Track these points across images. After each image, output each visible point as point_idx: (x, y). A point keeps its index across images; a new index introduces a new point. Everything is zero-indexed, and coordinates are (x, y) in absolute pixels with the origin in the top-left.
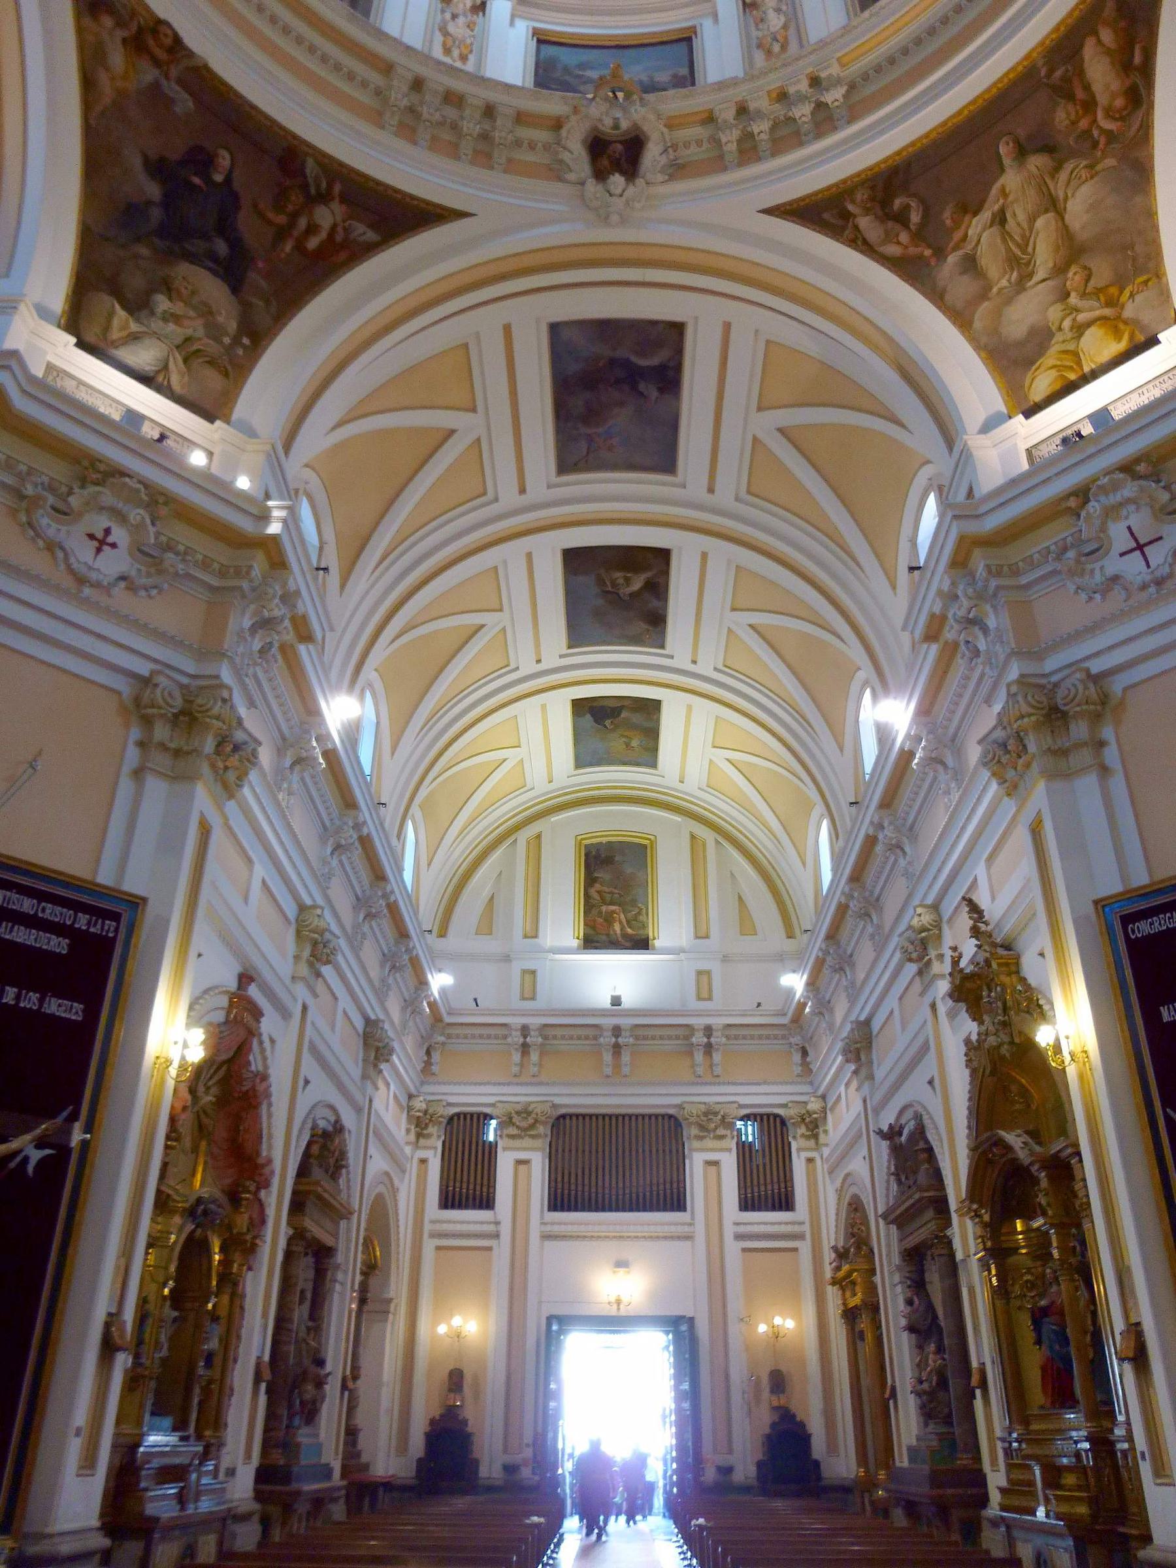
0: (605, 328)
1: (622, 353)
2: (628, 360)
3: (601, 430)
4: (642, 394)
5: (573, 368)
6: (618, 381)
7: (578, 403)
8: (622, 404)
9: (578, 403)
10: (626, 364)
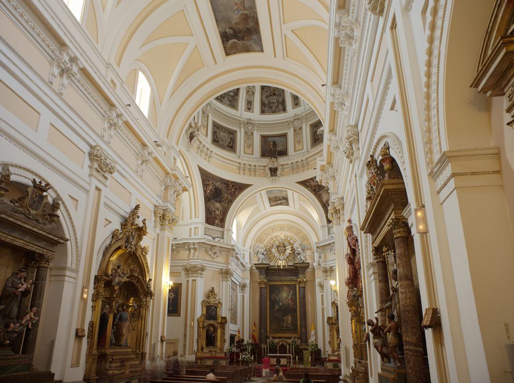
0: (247, 50)
1: (241, 43)
2: (239, 40)
3: (241, 12)
4: (231, 29)
5: (254, 37)
6: (240, 32)
7: (251, 24)
8: (237, 24)
9: (251, 24)
10: (239, 39)
